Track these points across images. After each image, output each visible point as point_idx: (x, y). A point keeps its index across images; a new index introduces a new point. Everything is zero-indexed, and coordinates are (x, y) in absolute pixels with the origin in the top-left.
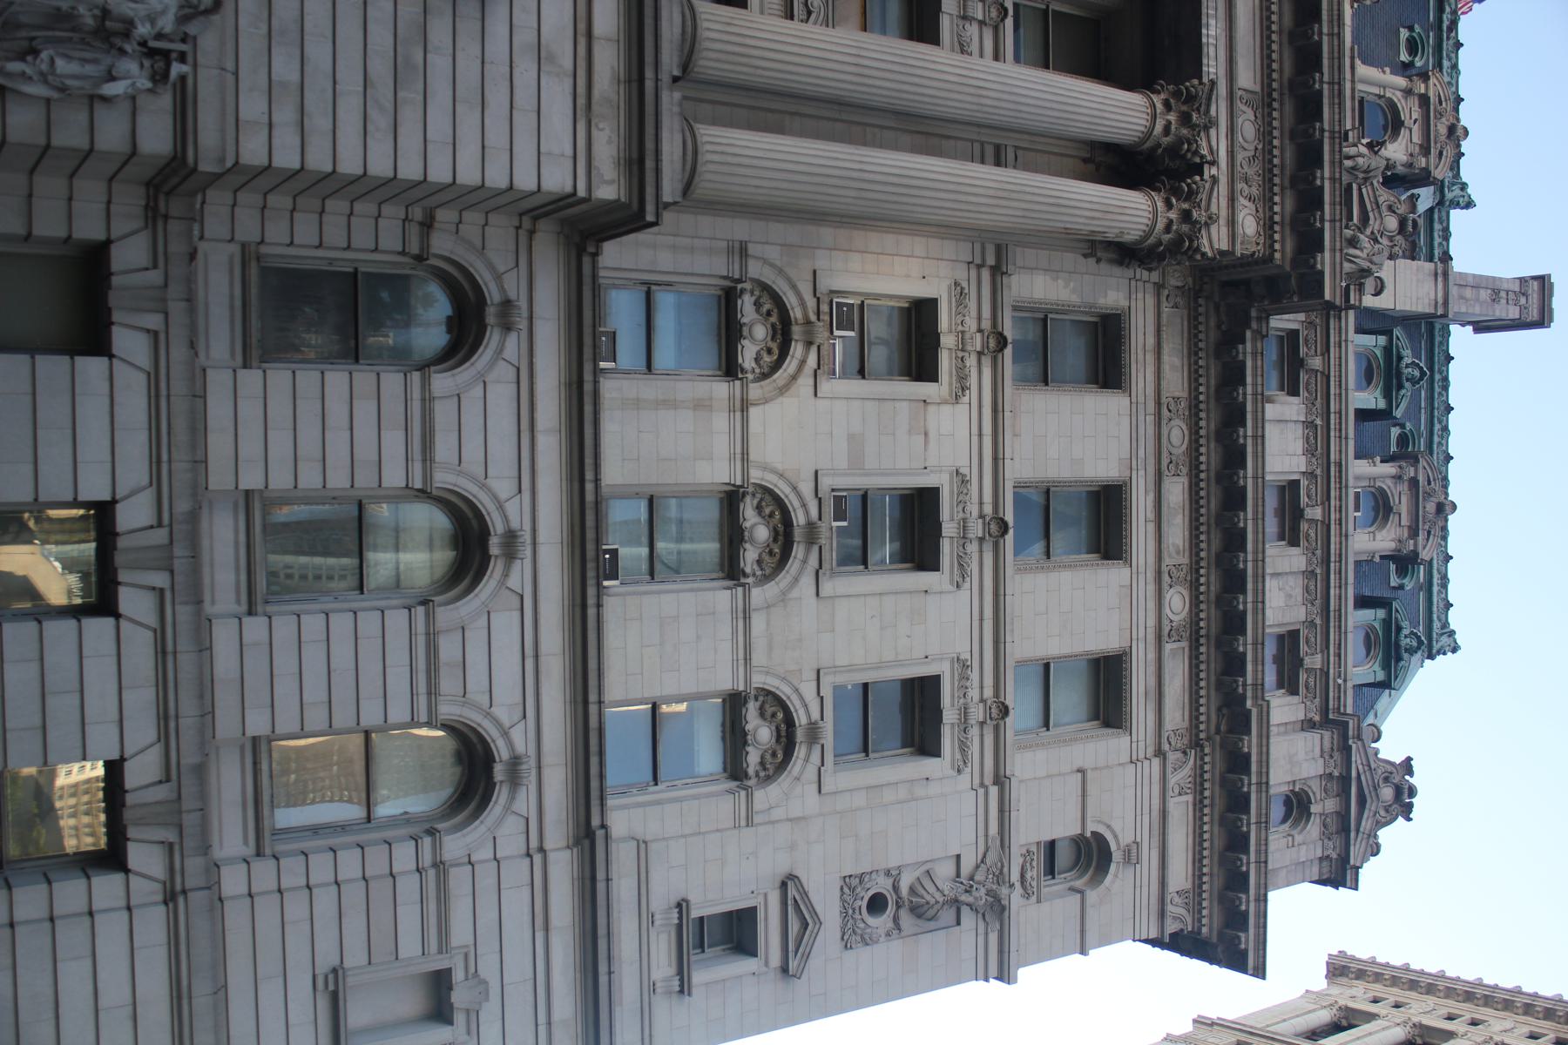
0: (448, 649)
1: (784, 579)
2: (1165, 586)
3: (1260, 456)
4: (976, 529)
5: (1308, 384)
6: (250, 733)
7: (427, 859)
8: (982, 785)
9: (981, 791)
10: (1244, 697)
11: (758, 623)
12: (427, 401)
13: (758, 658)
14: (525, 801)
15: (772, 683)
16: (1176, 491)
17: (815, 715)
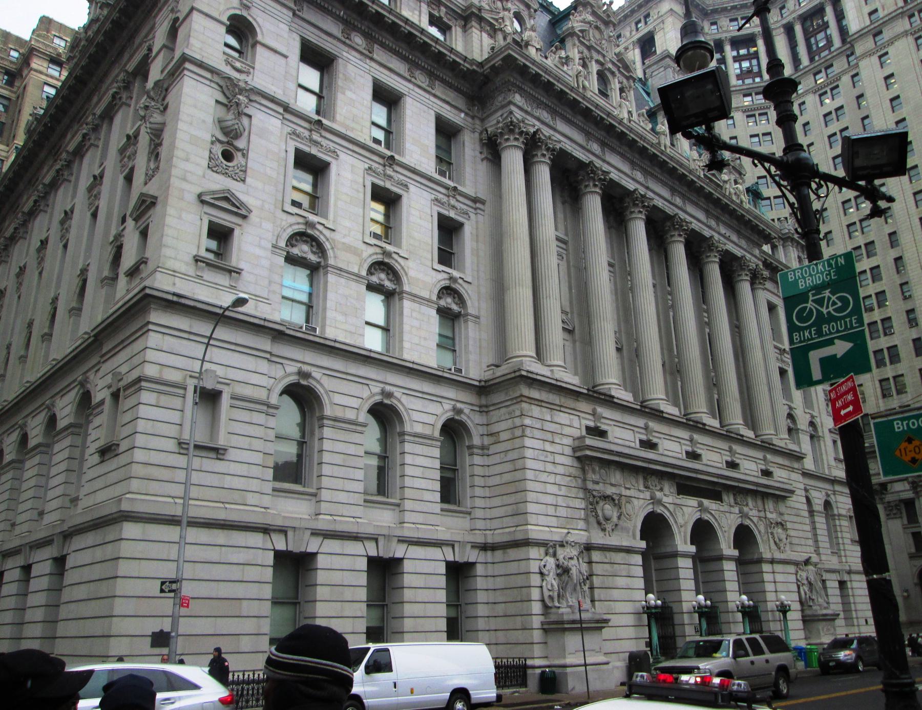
0: (419, 429)
1: (401, 273)
4: (389, 171)
6: (438, 511)
7: (480, 451)
8: (476, 209)
9: (479, 211)
11: (415, 291)
12: (335, 420)
13: (425, 294)
14: (466, 409)
15: (436, 291)
16: (379, 54)
17: (446, 276)
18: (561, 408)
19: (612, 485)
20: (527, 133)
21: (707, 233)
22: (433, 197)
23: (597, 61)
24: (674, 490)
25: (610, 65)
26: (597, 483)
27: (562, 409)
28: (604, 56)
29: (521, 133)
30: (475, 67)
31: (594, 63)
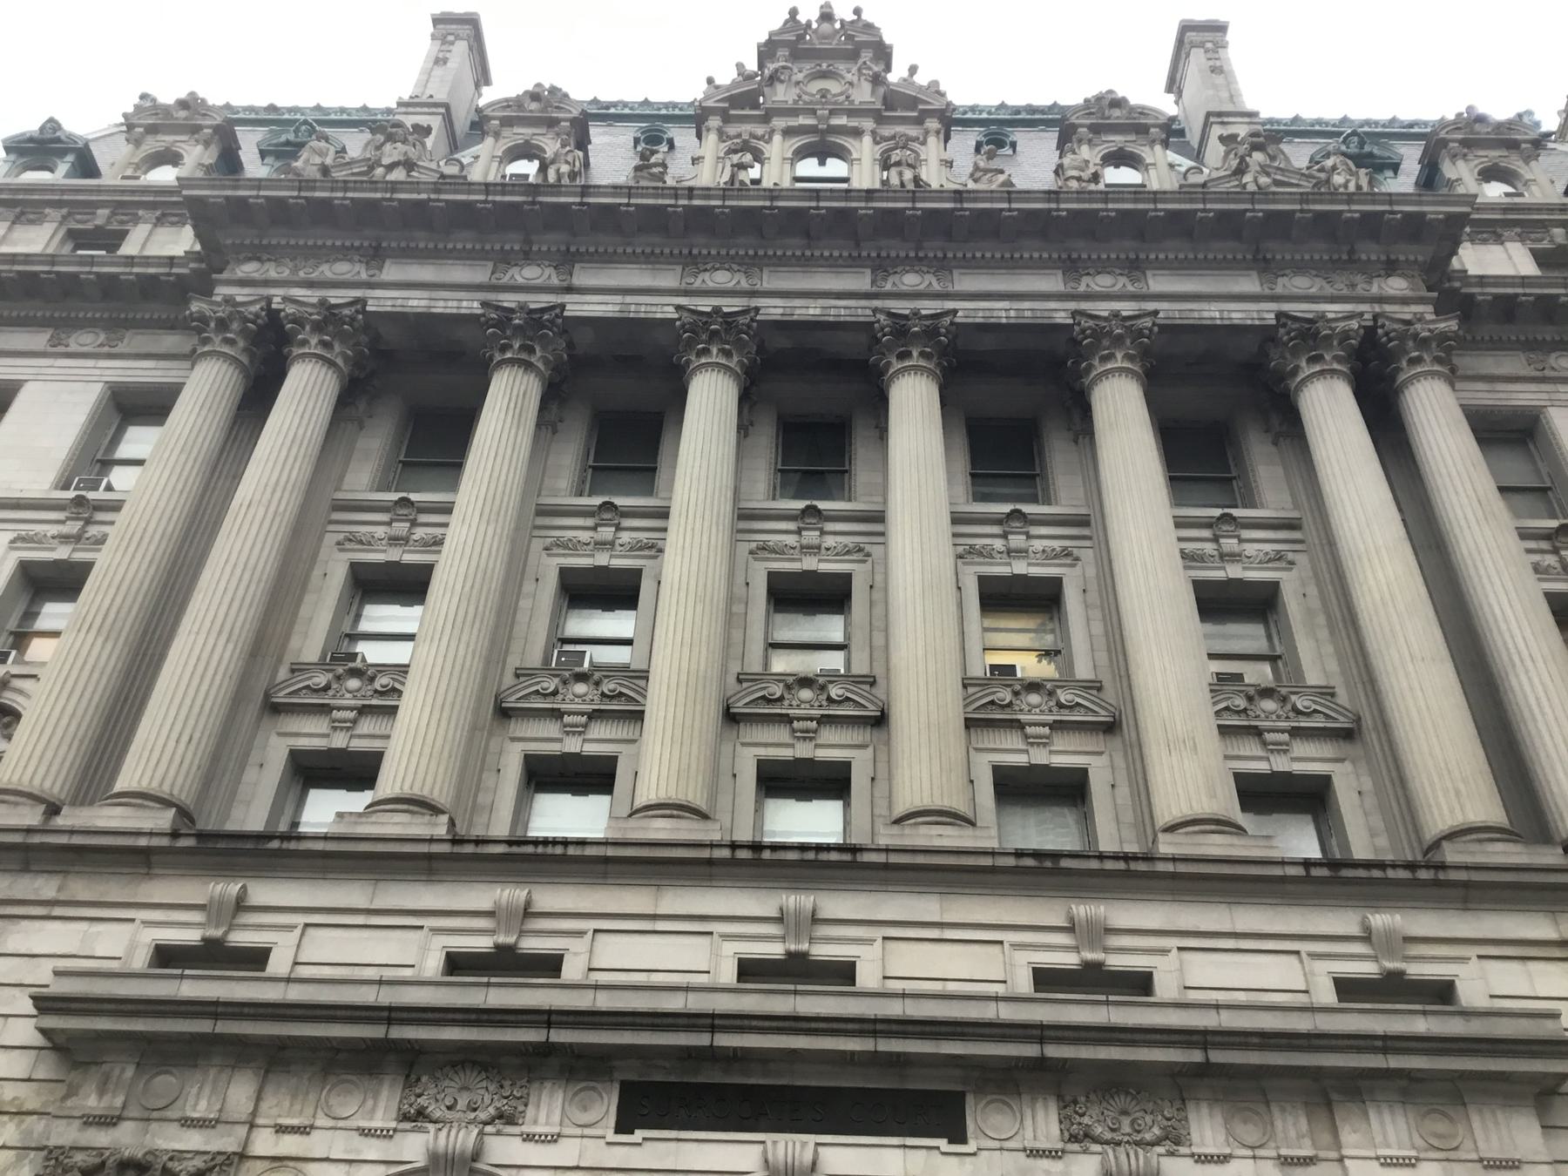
2: (69, 349)
3: (28, 258)
5: (79, 222)
10: (178, 275)
18: (49, 910)
19: (188, 1123)
20: (245, 320)
21: (1060, 313)
22: (11, 535)
23: (788, 132)
24: (606, 1107)
25: (841, 121)
26: (108, 1121)
27: (57, 911)
28: (813, 112)
29: (223, 325)
30: (192, 265)
31: (777, 138)
